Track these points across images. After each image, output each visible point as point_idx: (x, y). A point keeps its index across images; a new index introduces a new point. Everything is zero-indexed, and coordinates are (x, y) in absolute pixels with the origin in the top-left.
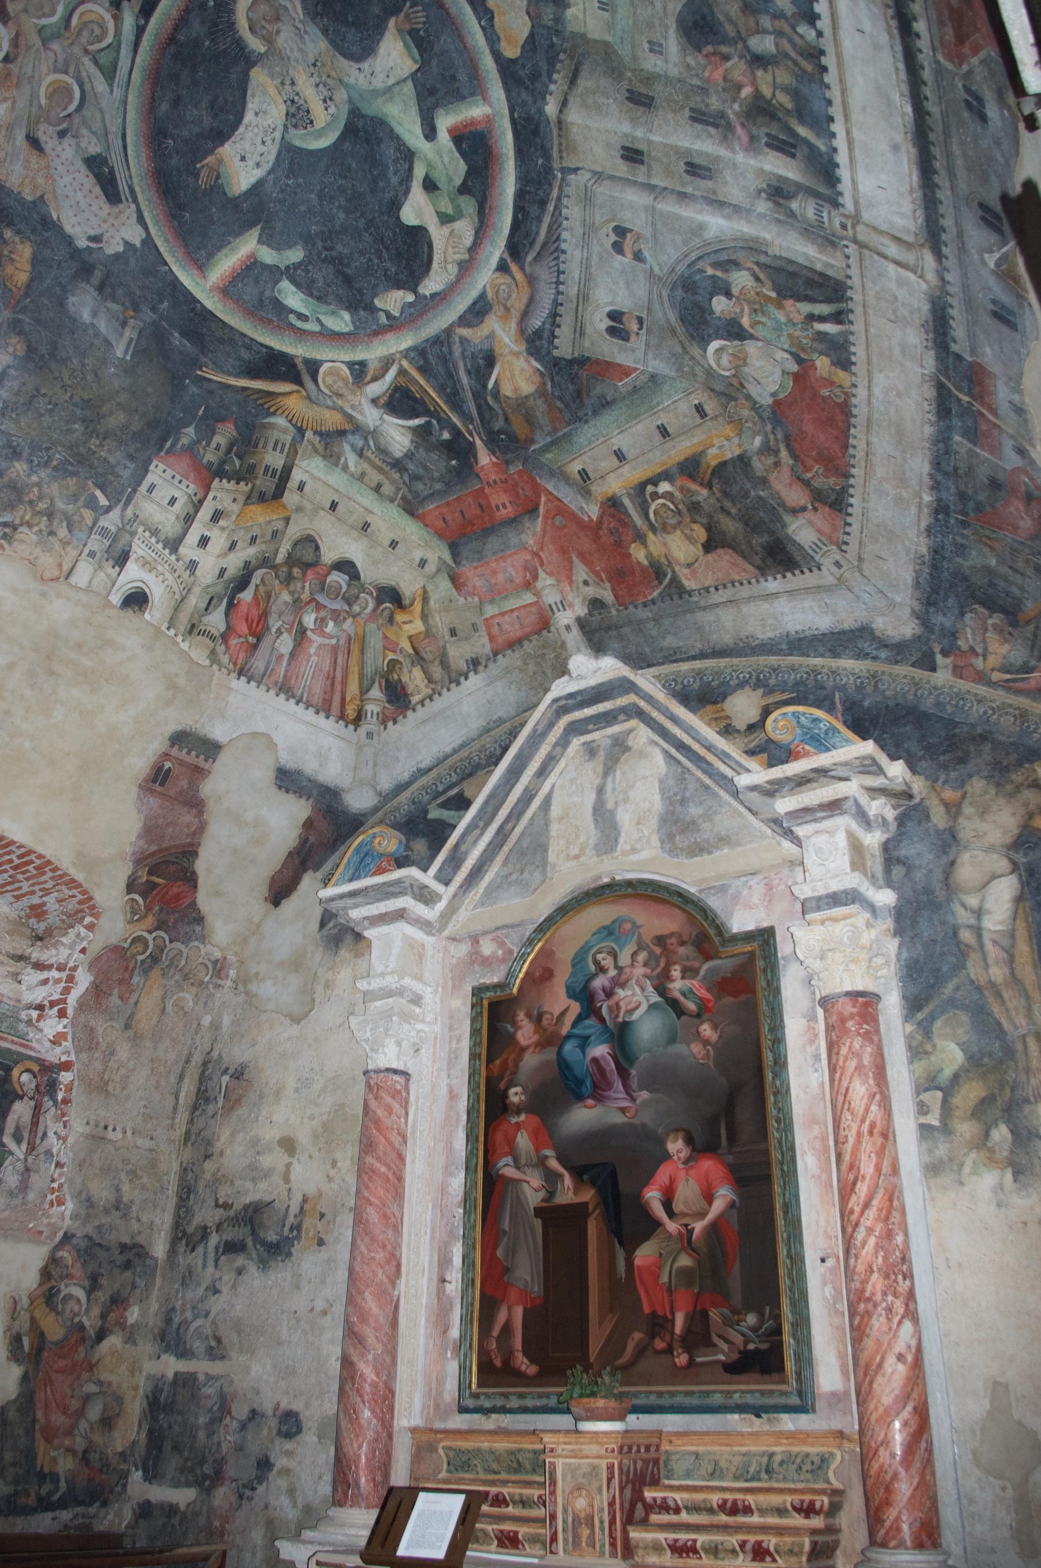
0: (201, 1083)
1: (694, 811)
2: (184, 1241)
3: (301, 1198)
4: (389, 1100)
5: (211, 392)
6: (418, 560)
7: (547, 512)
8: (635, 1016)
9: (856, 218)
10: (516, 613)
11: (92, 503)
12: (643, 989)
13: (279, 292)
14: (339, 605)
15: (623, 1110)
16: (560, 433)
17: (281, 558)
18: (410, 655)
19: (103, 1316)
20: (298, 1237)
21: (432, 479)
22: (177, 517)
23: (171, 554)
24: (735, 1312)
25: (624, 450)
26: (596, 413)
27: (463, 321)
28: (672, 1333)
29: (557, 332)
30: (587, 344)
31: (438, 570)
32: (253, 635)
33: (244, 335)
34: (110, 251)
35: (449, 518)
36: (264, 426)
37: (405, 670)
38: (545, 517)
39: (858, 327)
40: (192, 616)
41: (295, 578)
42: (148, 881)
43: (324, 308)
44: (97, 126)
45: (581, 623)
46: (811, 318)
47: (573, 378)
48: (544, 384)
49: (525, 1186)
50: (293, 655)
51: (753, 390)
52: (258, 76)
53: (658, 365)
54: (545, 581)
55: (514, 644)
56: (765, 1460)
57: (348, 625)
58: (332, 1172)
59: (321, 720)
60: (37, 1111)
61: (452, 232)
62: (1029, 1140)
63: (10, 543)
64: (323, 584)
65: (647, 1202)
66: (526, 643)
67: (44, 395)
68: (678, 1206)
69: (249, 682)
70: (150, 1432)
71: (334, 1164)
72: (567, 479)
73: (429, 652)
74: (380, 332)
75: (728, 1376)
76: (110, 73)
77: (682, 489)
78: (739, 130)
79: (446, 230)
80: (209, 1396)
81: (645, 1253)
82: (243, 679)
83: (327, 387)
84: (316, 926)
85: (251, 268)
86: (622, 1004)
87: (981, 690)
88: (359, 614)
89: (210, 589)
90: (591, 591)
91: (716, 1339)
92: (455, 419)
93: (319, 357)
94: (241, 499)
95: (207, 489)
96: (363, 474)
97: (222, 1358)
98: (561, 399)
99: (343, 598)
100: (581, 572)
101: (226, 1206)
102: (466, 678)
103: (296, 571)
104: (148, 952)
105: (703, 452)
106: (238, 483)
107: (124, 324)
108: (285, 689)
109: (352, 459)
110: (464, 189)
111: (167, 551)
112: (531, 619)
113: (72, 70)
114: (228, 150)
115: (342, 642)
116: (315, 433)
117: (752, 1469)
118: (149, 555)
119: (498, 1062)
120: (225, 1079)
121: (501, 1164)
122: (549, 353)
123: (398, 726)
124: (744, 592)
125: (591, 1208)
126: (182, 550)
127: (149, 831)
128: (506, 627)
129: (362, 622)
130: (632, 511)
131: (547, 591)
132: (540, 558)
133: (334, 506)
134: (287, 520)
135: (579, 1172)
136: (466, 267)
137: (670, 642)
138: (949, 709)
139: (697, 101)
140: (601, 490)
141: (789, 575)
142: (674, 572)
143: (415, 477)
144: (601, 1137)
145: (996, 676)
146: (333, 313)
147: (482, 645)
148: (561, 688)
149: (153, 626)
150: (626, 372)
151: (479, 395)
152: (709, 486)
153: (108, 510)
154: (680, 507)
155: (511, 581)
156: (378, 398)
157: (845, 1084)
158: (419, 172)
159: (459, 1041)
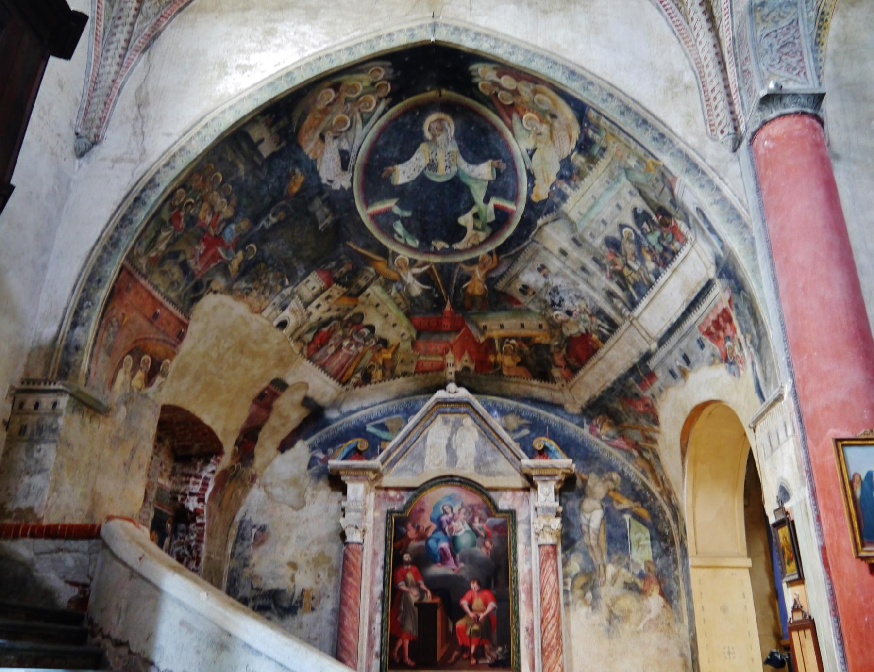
1: (489, 458)
9: (637, 318)
12: (463, 524)
14: (361, 341)
15: (453, 570)
17: (346, 318)
27: (466, 262)
31: (408, 339)
39: (615, 337)
44: (351, 140)
46: (600, 326)
50: (332, 355)
51: (564, 330)
52: (423, 146)
53: (532, 307)
55: (425, 372)
57: (361, 349)
58: (318, 580)
61: (476, 234)
68: (474, 607)
71: (319, 576)
72: (477, 327)
73: (388, 366)
74: (428, 252)
76: (365, 122)
77: (519, 345)
78: (608, 273)
79: (474, 232)
81: (460, 623)
85: (388, 213)
87: (598, 440)
90: (467, 364)
92: (443, 292)
94: (341, 293)
95: (329, 286)
100: (466, 357)
101: (258, 589)
107: (327, 217)
108: (323, 367)
109: (394, 291)
110: (490, 224)
113: (351, 115)
114: (400, 168)
116: (384, 278)
120: (254, 531)
124: (523, 381)
127: (250, 419)
133: (378, 305)
134: (356, 306)
135: (434, 593)
136: (475, 247)
137: (487, 388)
139: (598, 257)
140: (488, 334)
143: (417, 305)
144: (446, 578)
146: (413, 239)
147: (413, 368)
148: (440, 394)
150: (518, 303)
152: (530, 348)
153: (288, 287)
158: (474, 209)
159: (378, 530)
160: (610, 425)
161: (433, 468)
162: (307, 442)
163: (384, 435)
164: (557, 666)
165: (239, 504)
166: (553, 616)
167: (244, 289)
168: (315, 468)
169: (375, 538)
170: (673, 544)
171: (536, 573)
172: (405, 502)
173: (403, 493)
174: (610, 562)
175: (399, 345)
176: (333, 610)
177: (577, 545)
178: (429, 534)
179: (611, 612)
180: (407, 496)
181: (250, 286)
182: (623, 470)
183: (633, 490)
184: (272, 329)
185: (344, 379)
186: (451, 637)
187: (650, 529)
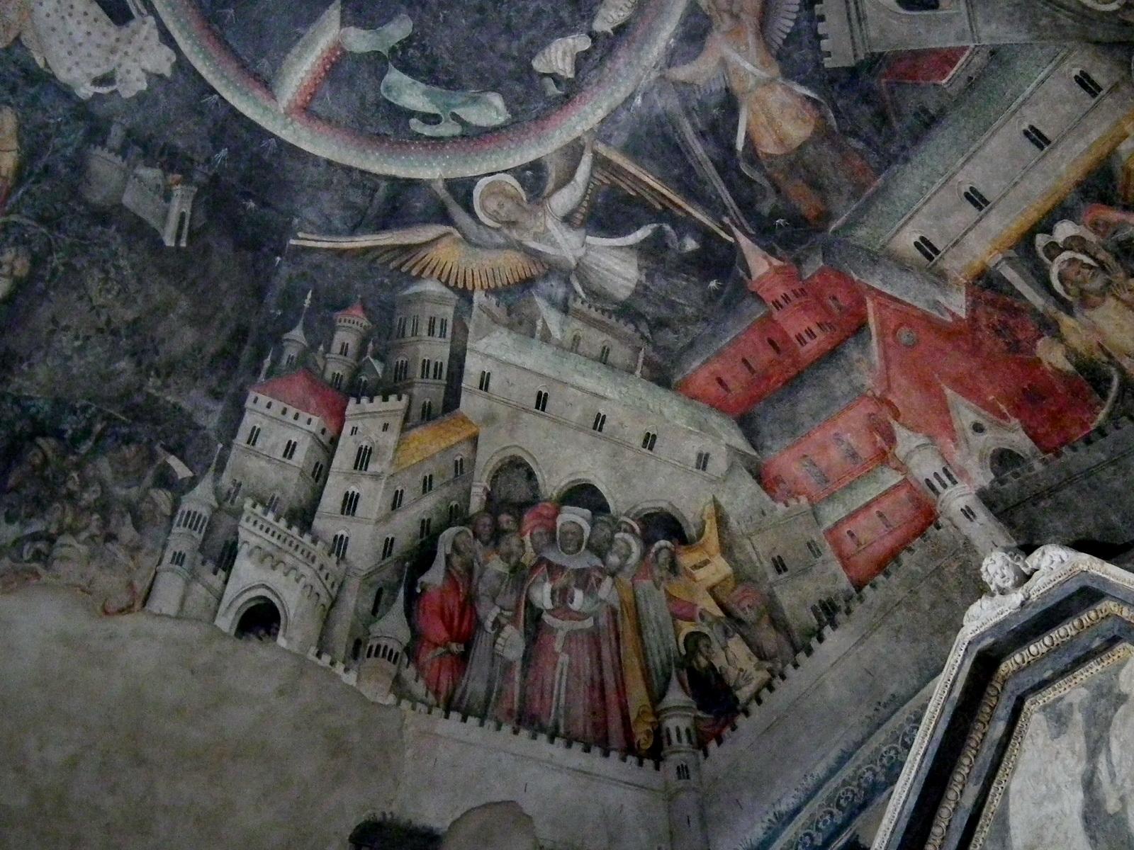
5: (317, 267)
6: (693, 457)
7: (882, 324)
10: (874, 510)
11: (165, 479)
13: (388, 89)
14: (585, 560)
16: (870, 191)
17: (476, 504)
18: (717, 619)
21: (685, 320)
22: (302, 473)
23: (301, 534)
25: (981, 189)
26: (916, 139)
27: (672, 58)
29: (822, 28)
30: (873, 33)
31: (732, 467)
32: (457, 640)
33: (349, 170)
34: (127, 94)
35: (726, 377)
36: (408, 301)
37: (716, 646)
38: (882, 335)
40: (353, 626)
41: (505, 532)
43: (459, 97)
45: (985, 497)
47: (867, 97)
48: (823, 117)
50: (527, 658)
53: (994, 31)
54: (906, 441)
55: (886, 562)
57: (606, 589)
59: (594, 760)
63: (47, 565)
64: (552, 531)
66: (905, 557)
67: (67, 328)
69: (464, 720)
77: (1095, 226)
82: (455, 716)
83: (490, 216)
88: (620, 568)
89: (374, 578)
90: (990, 440)
92: (699, 215)
93: (469, 173)
94: (396, 423)
95: (340, 418)
96: (576, 339)
98: (854, 134)
99: (589, 547)
100: (965, 413)
102: (821, 639)
103: (504, 519)
105: (1113, 152)
106: (385, 399)
107: (167, 197)
109: (553, 319)
111: (295, 530)
112: (899, 510)
115: (603, 621)
116: (489, 291)
118: (266, 541)
122: (819, 65)
123: (726, 747)
126: (318, 524)
128: (864, 536)
129: (628, 582)
130: (1021, 286)
131: (916, 459)
132: (890, 404)
133: (542, 400)
134: (474, 440)
140: (959, 265)
142: (1122, 371)
143: (660, 324)
146: (475, 100)
149: (295, 654)
150: (947, 58)
151: (726, 164)
153: (193, 482)
154: (1101, 256)
155: (854, 455)
156: (573, 212)
167: (18, 543)
175: (715, 501)
181: (37, 526)
184: (228, 645)
185: (642, 735)
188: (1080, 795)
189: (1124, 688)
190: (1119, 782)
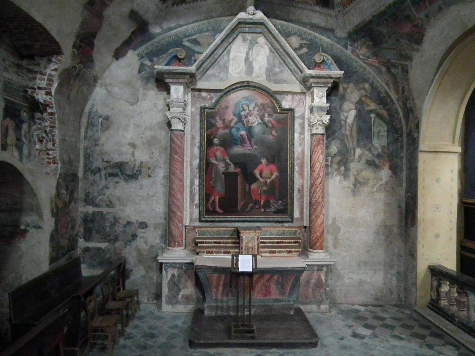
0: (89, 119)
1: (277, 70)
2: (90, 171)
3: (140, 163)
4: (180, 139)
8: (254, 125)
12: (256, 118)
19: (70, 197)
20: (140, 174)
24: (276, 200)
28: (260, 204)
42: (79, 45)
49: (219, 166)
56: (283, 232)
58: (152, 156)
60: (30, 127)
62: (348, 170)
65: (255, 173)
68: (264, 175)
70: (85, 229)
71: (152, 153)
75: (274, 214)
80: (109, 218)
81: (254, 186)
84: (136, 72)
86: (250, 121)
87: (357, 59)
91: (271, 206)
97: (113, 207)
101: (107, 162)
104: (76, 73)
117: (279, 234)
119: (210, 130)
120: (100, 120)
121: (211, 159)
124: (309, 7)
125: (239, 173)
127: (84, 24)
135: (236, 164)
138: (348, 62)
141: (324, 8)
144: (245, 155)
145: (361, 57)
148: (242, 15)
157: (318, 155)
160: (368, 47)
161: (235, 75)
162: (136, 52)
163: (197, 48)
164: (322, 215)
165: (86, 100)
166: (320, 183)
168: (144, 73)
169: (192, 127)
170: (402, 135)
171: (307, 153)
172: (214, 101)
173: (212, 94)
174: (358, 146)
176: (164, 177)
177: (337, 134)
178: (232, 125)
179: (356, 179)
180: (215, 97)
182: (373, 83)
183: (379, 96)
186: (248, 195)
187: (387, 124)
188: (245, 55)
189: (258, 41)
190: (253, 56)
